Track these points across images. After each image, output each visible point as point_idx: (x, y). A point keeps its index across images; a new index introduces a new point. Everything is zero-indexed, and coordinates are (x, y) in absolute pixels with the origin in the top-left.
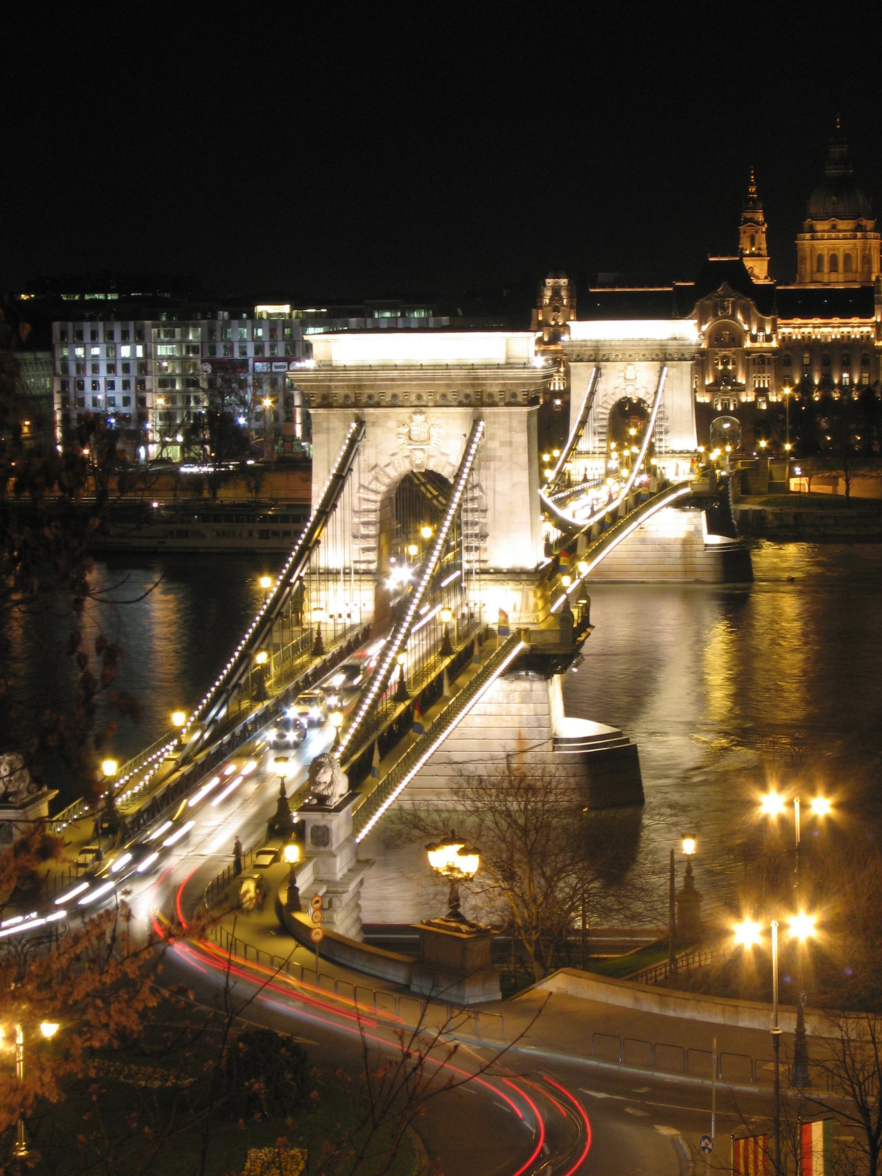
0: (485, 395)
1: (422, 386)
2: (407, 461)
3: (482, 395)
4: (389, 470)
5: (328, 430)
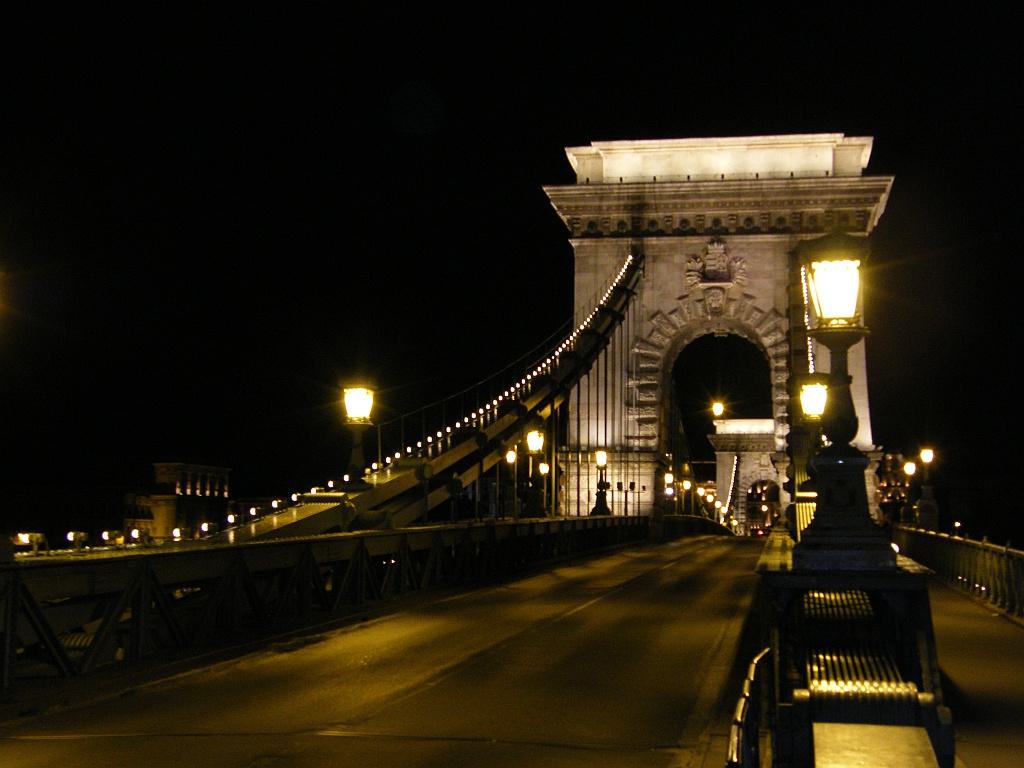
0: (805, 219)
1: (723, 205)
2: (699, 305)
3: (801, 220)
4: (673, 317)
5: (596, 268)
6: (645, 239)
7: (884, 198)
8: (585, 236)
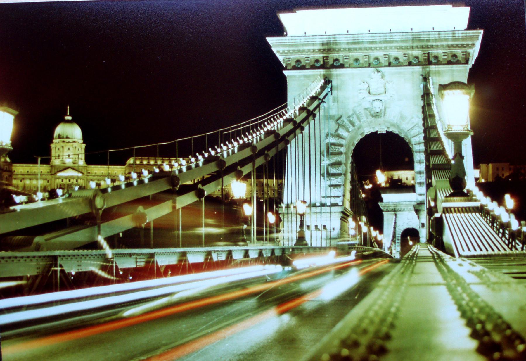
0: (430, 56)
6: (332, 70)
7: (478, 43)
8: (294, 68)
